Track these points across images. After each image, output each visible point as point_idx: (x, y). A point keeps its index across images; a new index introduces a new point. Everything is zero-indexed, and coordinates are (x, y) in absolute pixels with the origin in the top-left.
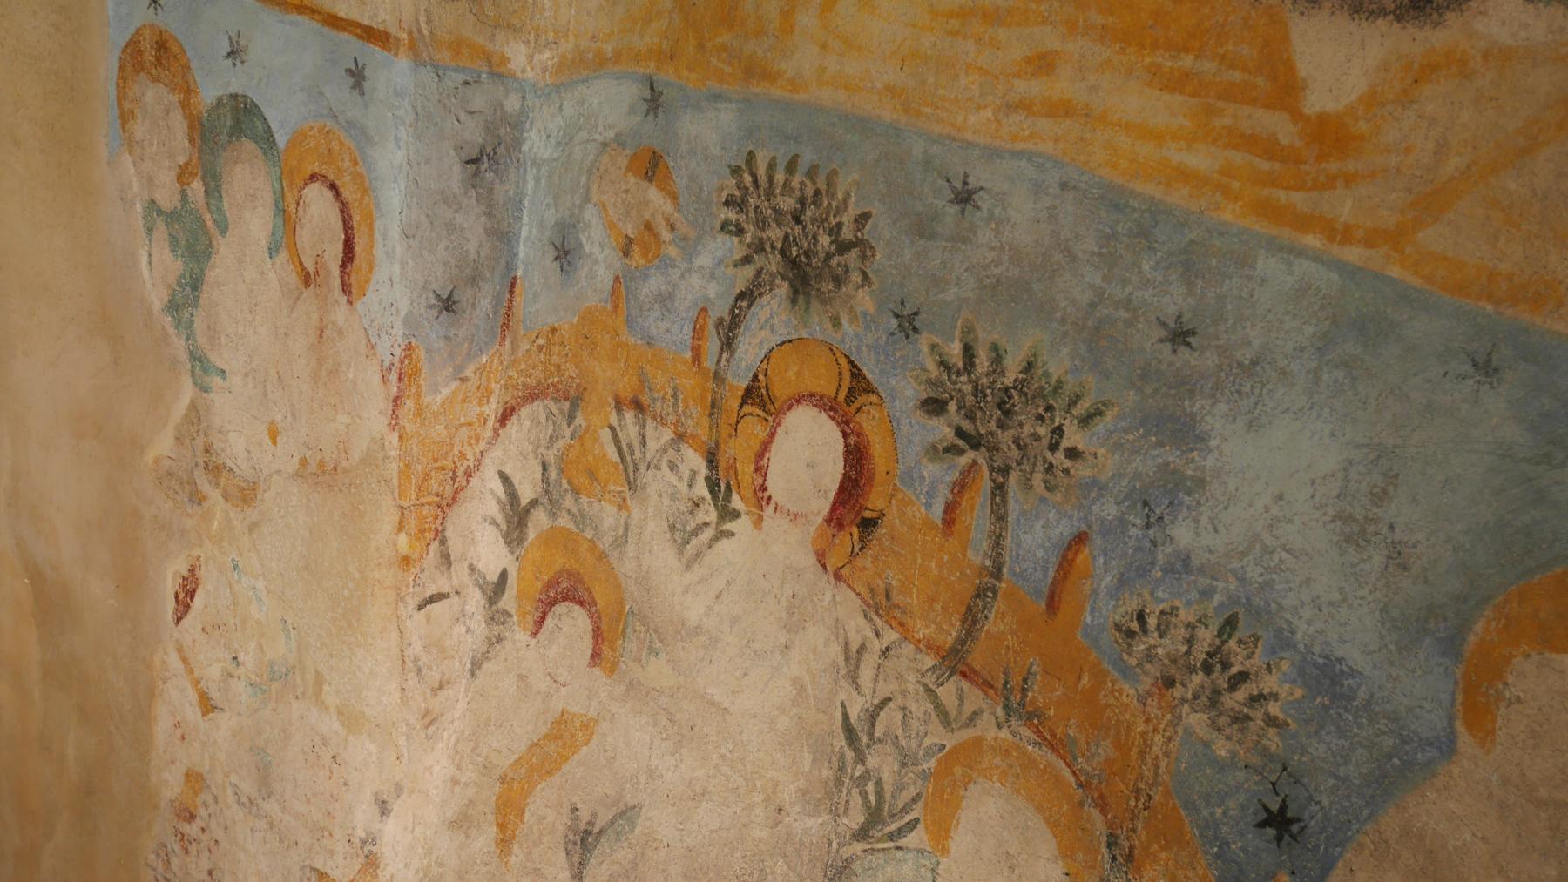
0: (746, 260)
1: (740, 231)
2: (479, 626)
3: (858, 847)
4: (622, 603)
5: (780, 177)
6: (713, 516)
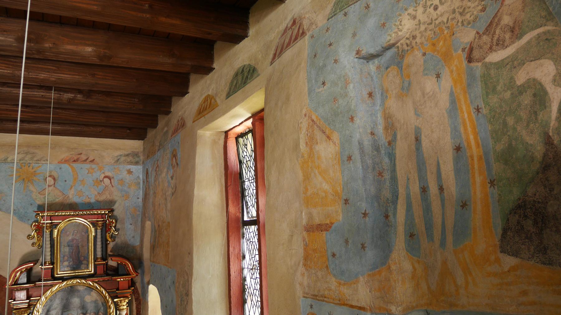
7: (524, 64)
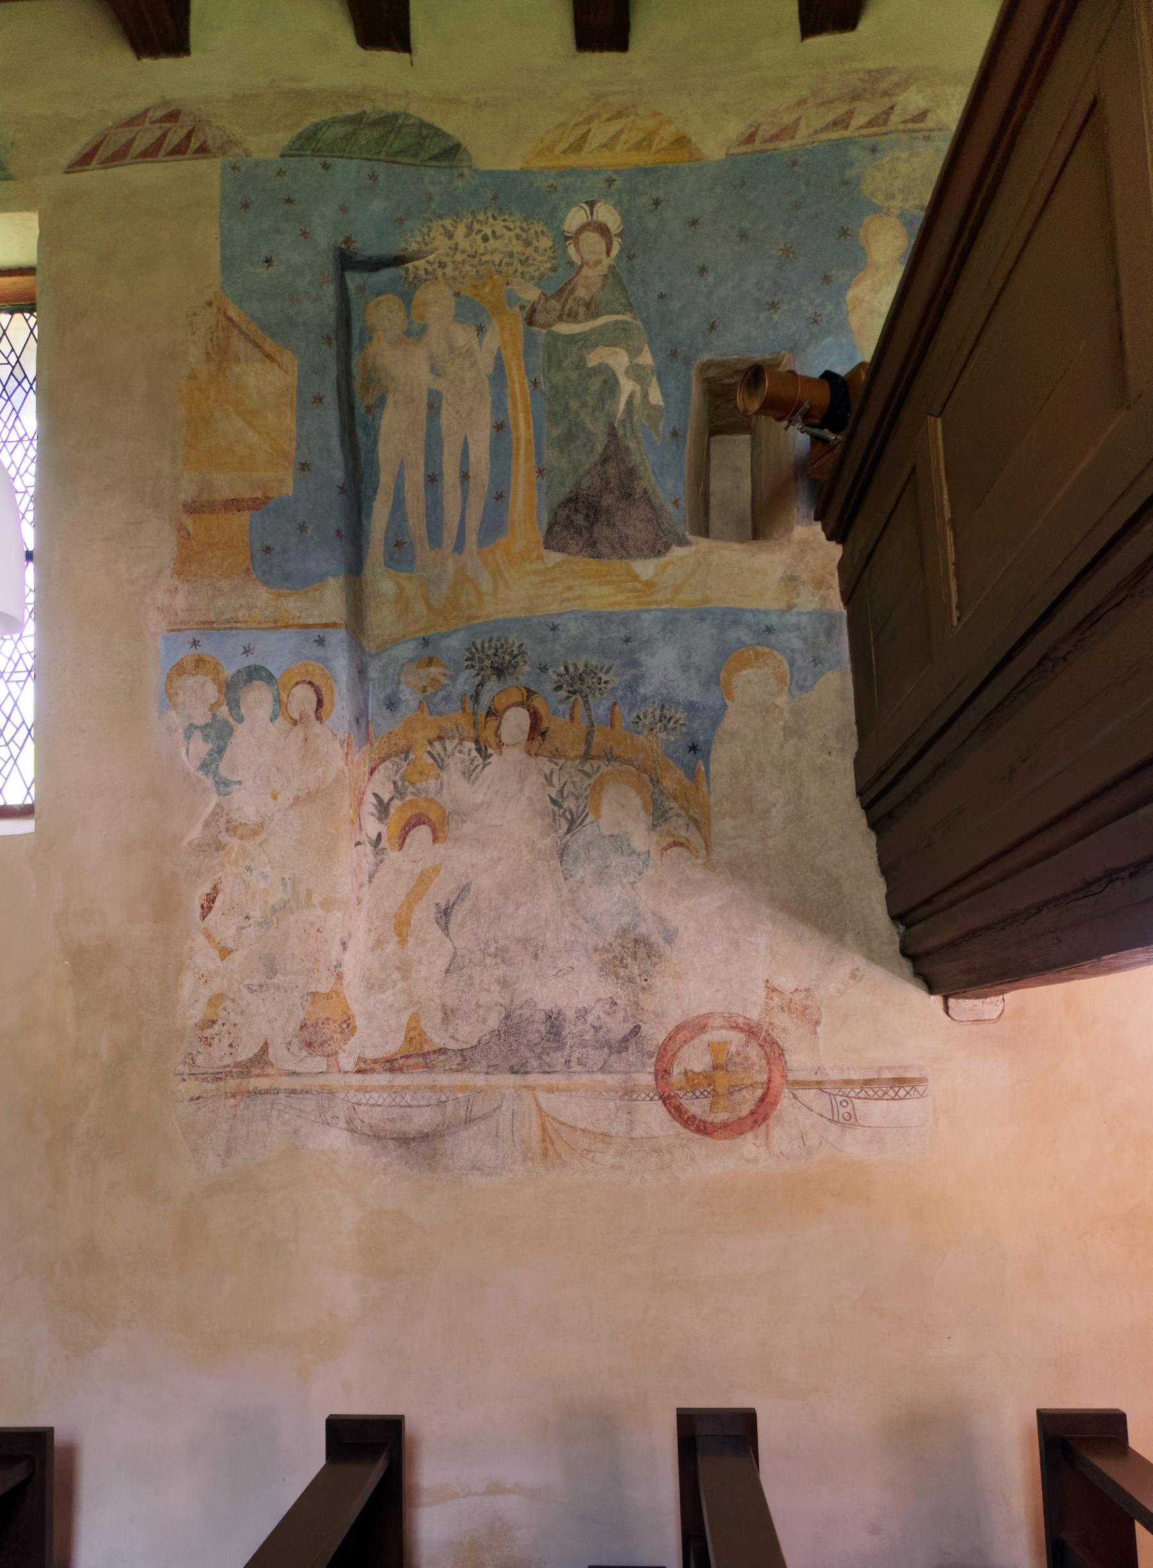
0: (478, 674)
1: (473, 667)
2: (372, 859)
3: (568, 836)
4: (444, 813)
5: (486, 645)
6: (481, 760)
7: (597, 346)
